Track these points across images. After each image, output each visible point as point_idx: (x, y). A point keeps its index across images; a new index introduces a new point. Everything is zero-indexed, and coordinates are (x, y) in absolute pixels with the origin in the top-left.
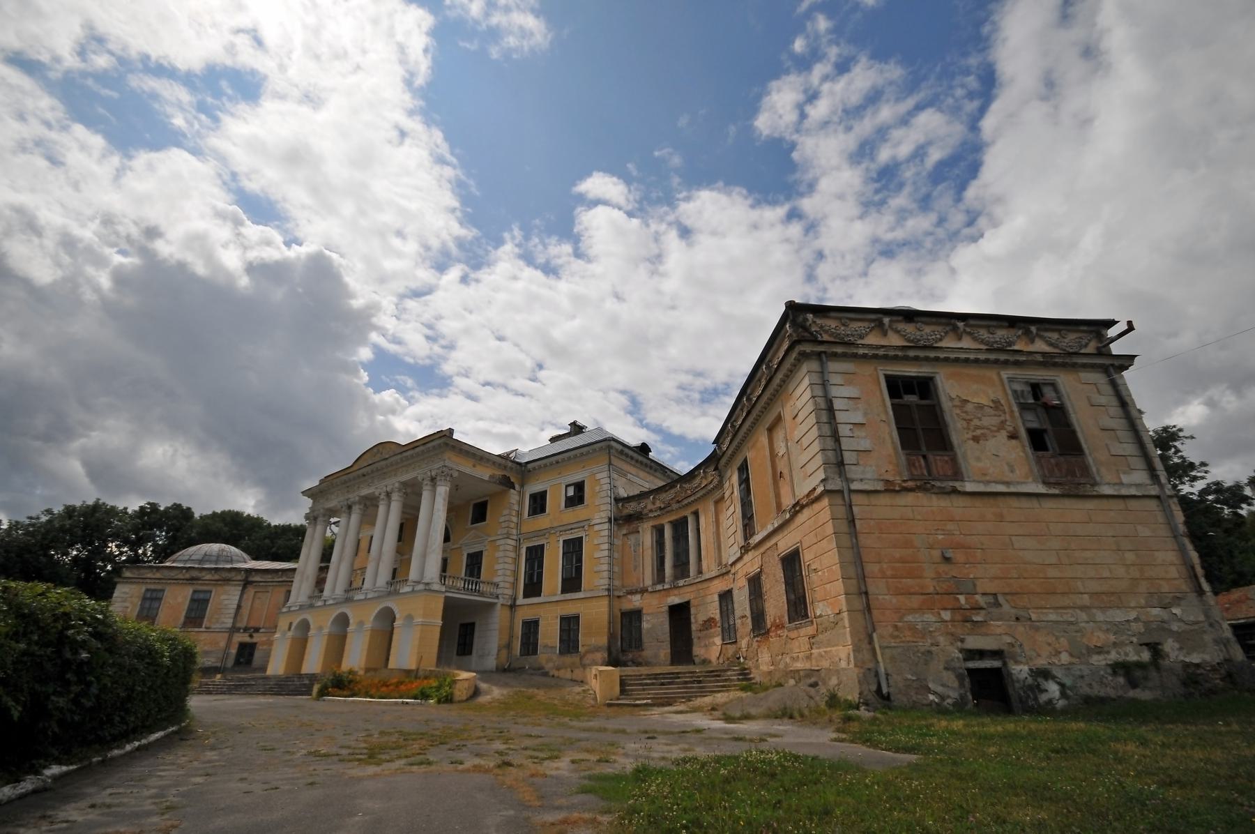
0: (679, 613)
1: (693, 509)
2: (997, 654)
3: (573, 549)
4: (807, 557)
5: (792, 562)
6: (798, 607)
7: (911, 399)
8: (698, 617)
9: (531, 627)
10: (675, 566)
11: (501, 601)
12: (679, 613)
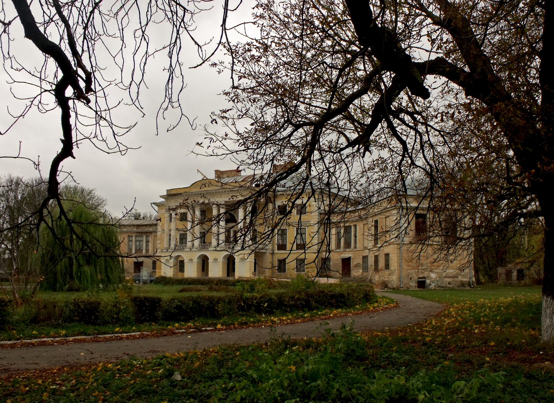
0: (346, 262)
1: (355, 223)
2: (424, 278)
3: (300, 232)
4: (391, 256)
5: (387, 255)
6: (387, 266)
7: (420, 220)
8: (353, 263)
9: (282, 263)
10: (345, 244)
11: (269, 251)
12: (346, 262)
